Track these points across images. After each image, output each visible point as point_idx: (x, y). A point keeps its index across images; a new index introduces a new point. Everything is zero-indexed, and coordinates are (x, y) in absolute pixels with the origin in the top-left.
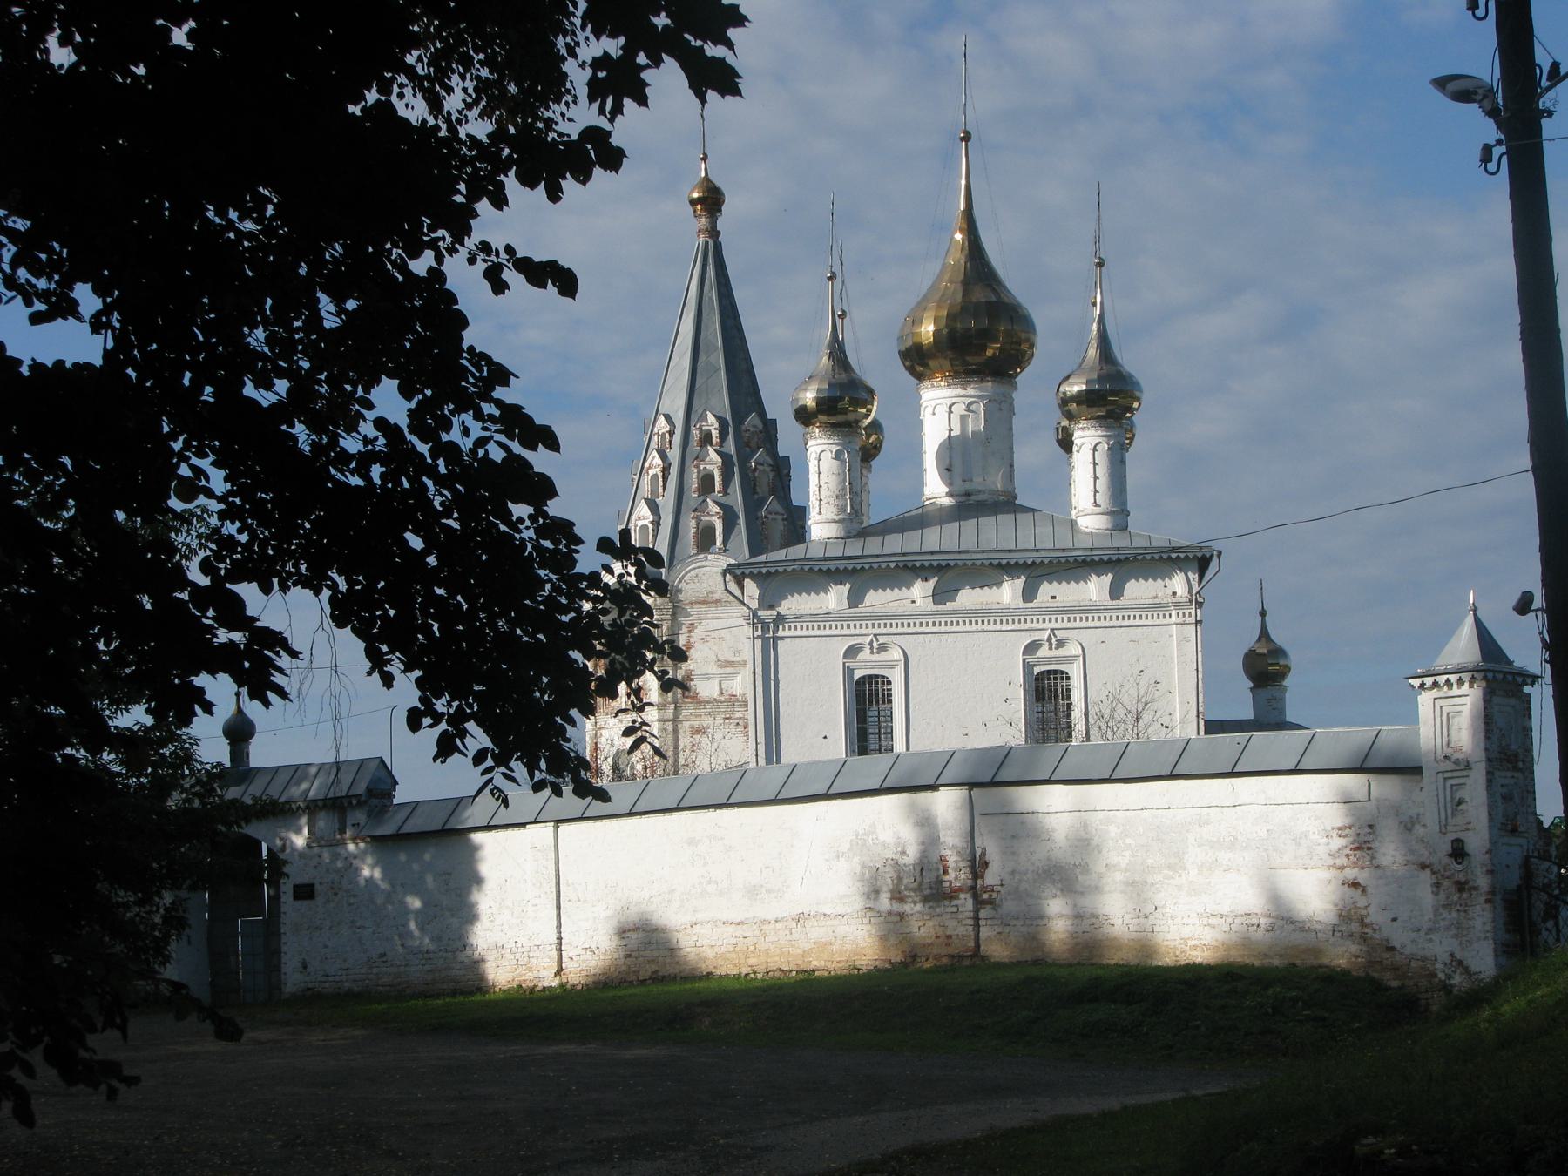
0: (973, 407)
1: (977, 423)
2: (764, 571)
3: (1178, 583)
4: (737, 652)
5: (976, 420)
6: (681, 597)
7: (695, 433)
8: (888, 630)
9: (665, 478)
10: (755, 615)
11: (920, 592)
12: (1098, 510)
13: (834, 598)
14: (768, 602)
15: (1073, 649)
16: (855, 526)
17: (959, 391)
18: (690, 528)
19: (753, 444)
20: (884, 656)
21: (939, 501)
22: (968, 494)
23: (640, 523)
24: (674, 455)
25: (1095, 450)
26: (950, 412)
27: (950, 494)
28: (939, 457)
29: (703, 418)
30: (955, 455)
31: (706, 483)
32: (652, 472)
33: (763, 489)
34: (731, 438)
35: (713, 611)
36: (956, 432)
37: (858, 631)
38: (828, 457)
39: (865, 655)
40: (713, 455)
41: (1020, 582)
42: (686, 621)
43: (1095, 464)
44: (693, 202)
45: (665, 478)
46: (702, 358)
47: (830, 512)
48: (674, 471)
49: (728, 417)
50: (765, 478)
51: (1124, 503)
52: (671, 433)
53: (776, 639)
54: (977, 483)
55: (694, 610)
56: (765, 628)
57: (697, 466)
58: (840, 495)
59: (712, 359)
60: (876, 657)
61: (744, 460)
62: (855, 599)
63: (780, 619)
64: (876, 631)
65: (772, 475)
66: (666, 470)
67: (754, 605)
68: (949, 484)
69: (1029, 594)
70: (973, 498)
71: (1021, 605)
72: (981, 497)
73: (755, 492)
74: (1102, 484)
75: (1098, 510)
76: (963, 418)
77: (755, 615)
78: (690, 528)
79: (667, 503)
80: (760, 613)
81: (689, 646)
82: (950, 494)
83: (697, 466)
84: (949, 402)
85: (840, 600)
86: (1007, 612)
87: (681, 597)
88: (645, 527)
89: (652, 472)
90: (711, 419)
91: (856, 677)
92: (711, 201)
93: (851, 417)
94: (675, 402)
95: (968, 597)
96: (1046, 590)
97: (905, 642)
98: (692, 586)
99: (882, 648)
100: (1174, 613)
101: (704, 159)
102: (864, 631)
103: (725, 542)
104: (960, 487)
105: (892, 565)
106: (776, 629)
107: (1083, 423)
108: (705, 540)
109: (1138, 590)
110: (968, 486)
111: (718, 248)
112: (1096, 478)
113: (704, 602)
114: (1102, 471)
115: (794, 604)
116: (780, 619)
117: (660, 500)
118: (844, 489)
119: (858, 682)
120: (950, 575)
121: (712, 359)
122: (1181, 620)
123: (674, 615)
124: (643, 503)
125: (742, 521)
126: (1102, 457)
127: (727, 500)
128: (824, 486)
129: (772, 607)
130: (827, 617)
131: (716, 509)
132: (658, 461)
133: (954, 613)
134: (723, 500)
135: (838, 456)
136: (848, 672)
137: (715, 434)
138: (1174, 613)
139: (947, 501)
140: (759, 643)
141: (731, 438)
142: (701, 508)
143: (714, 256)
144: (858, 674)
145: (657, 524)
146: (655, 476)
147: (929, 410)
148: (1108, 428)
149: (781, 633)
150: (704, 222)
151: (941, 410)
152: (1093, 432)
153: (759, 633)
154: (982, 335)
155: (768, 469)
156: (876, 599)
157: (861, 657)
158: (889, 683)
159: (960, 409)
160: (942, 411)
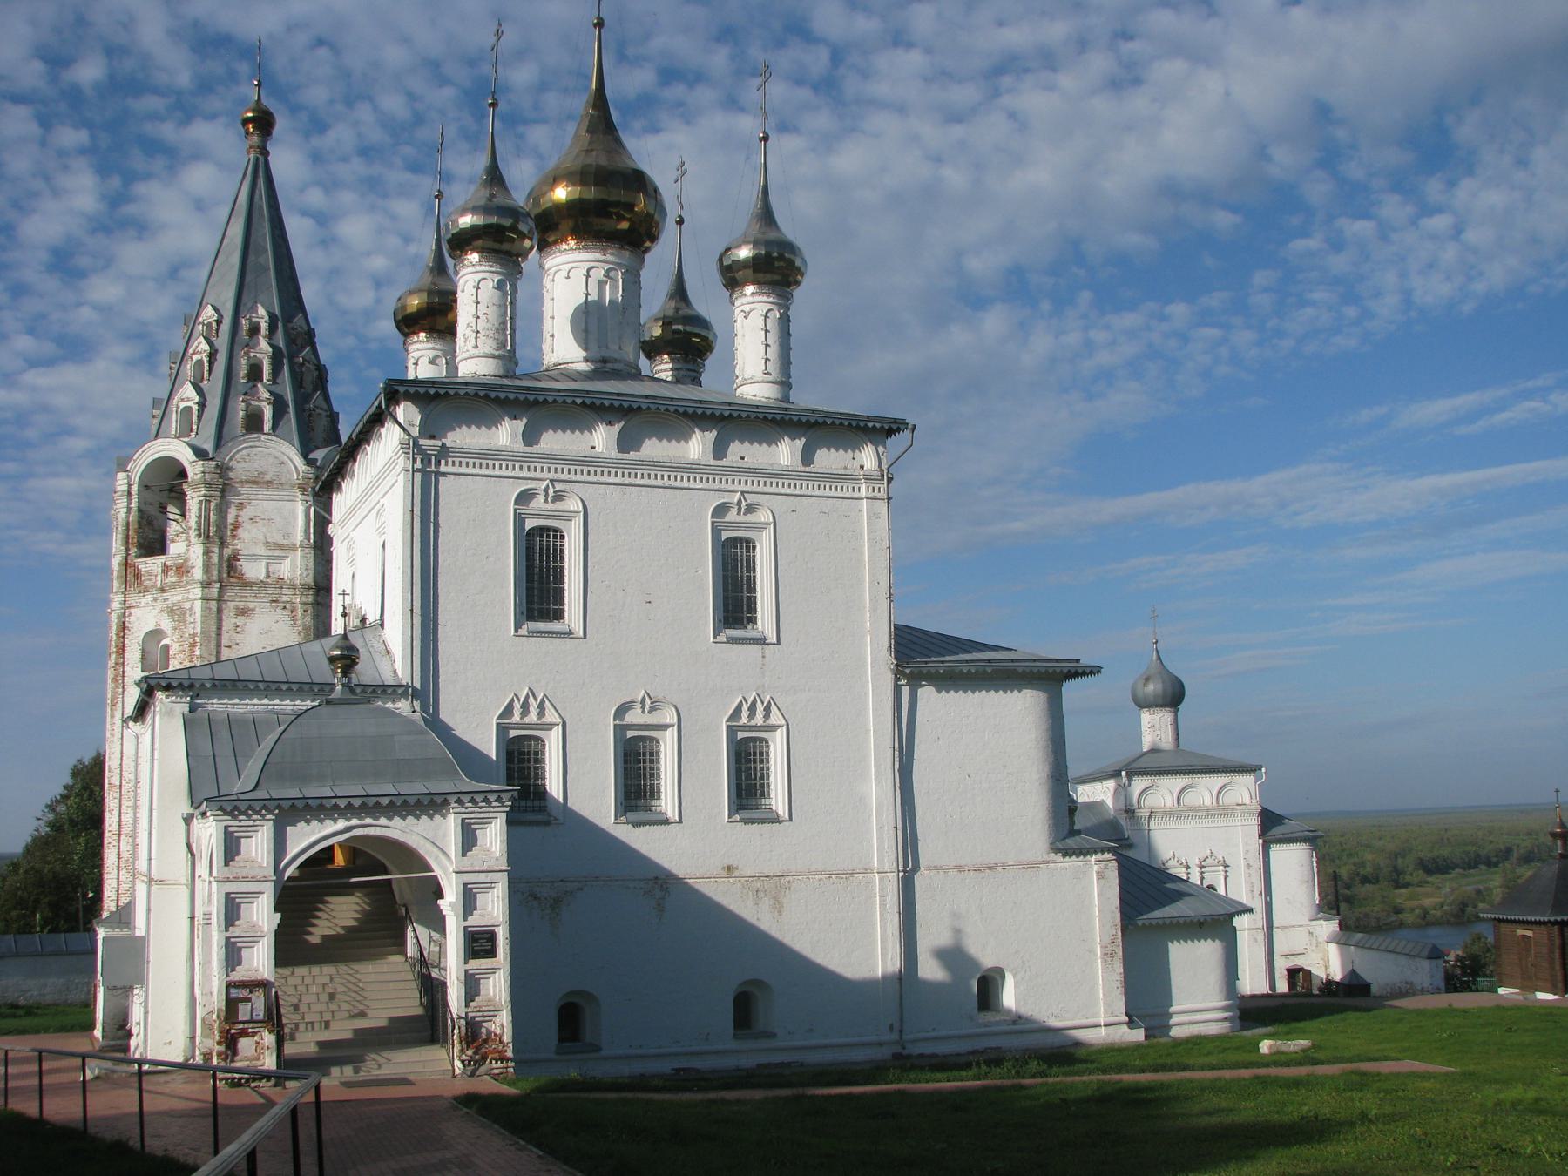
0: (612, 274)
1: (614, 293)
2: (432, 391)
3: (868, 457)
4: (287, 535)
5: (614, 288)
6: (231, 475)
8: (565, 476)
11: (602, 438)
13: (506, 434)
14: (429, 430)
15: (763, 516)
17: (598, 256)
18: (239, 411)
19: (299, 342)
20: (559, 506)
22: (604, 361)
23: (182, 405)
24: (222, 343)
25: (766, 317)
26: (588, 276)
27: (586, 360)
28: (574, 321)
30: (588, 320)
31: (255, 373)
32: (195, 358)
33: (308, 387)
34: (280, 333)
35: (264, 492)
36: (594, 297)
37: (531, 474)
38: (488, 287)
39: (538, 503)
40: (264, 344)
41: (711, 436)
42: (235, 499)
44: (246, 122)
45: (211, 364)
46: (252, 258)
47: (488, 346)
48: (222, 359)
49: (277, 311)
50: (310, 377)
52: (219, 322)
53: (439, 474)
54: (613, 351)
55: (245, 489)
56: (426, 460)
57: (247, 353)
58: (500, 329)
59: (261, 260)
60: (550, 506)
61: (292, 358)
62: (530, 437)
63: (444, 452)
64: (552, 475)
65: (316, 374)
66: (212, 356)
67: (415, 432)
68: (586, 349)
69: (719, 450)
70: (609, 365)
71: (712, 462)
72: (616, 366)
73: (301, 386)
74: (773, 352)
76: (601, 284)
78: (239, 411)
80: (422, 442)
81: (236, 526)
82: (586, 360)
83: (247, 353)
84: (588, 265)
85: (514, 435)
86: (695, 468)
87: (231, 475)
88: (189, 409)
89: (195, 358)
90: (262, 311)
91: (528, 527)
93: (515, 248)
95: (653, 448)
96: (736, 449)
97: (588, 492)
98: (242, 465)
99: (558, 497)
100: (864, 487)
102: (539, 475)
103: (274, 427)
105: (579, 401)
106: (438, 464)
107: (750, 289)
108: (253, 423)
109: (829, 459)
110: (607, 354)
112: (767, 345)
113: (255, 483)
114: (773, 339)
115: (463, 437)
116: (444, 452)
118: (504, 323)
119: (528, 534)
120: (639, 418)
121: (261, 260)
122: (870, 494)
123: (223, 491)
124: (189, 386)
125: (291, 410)
128: (483, 318)
129: (433, 437)
130: (498, 455)
131: (267, 395)
132: (205, 346)
133: (639, 464)
134: (273, 388)
135: (500, 286)
136: (520, 520)
137: (264, 326)
138: (864, 487)
139: (584, 367)
140: (418, 476)
141: (280, 333)
142: (250, 392)
143: (261, 173)
144: (530, 524)
145: (202, 405)
146: (200, 362)
148: (779, 296)
149: (443, 469)
150: (255, 139)
151: (569, 276)
152: (765, 299)
153: (418, 465)
154: (616, 210)
156: (553, 441)
157: (534, 504)
158: (563, 537)
159: (599, 274)
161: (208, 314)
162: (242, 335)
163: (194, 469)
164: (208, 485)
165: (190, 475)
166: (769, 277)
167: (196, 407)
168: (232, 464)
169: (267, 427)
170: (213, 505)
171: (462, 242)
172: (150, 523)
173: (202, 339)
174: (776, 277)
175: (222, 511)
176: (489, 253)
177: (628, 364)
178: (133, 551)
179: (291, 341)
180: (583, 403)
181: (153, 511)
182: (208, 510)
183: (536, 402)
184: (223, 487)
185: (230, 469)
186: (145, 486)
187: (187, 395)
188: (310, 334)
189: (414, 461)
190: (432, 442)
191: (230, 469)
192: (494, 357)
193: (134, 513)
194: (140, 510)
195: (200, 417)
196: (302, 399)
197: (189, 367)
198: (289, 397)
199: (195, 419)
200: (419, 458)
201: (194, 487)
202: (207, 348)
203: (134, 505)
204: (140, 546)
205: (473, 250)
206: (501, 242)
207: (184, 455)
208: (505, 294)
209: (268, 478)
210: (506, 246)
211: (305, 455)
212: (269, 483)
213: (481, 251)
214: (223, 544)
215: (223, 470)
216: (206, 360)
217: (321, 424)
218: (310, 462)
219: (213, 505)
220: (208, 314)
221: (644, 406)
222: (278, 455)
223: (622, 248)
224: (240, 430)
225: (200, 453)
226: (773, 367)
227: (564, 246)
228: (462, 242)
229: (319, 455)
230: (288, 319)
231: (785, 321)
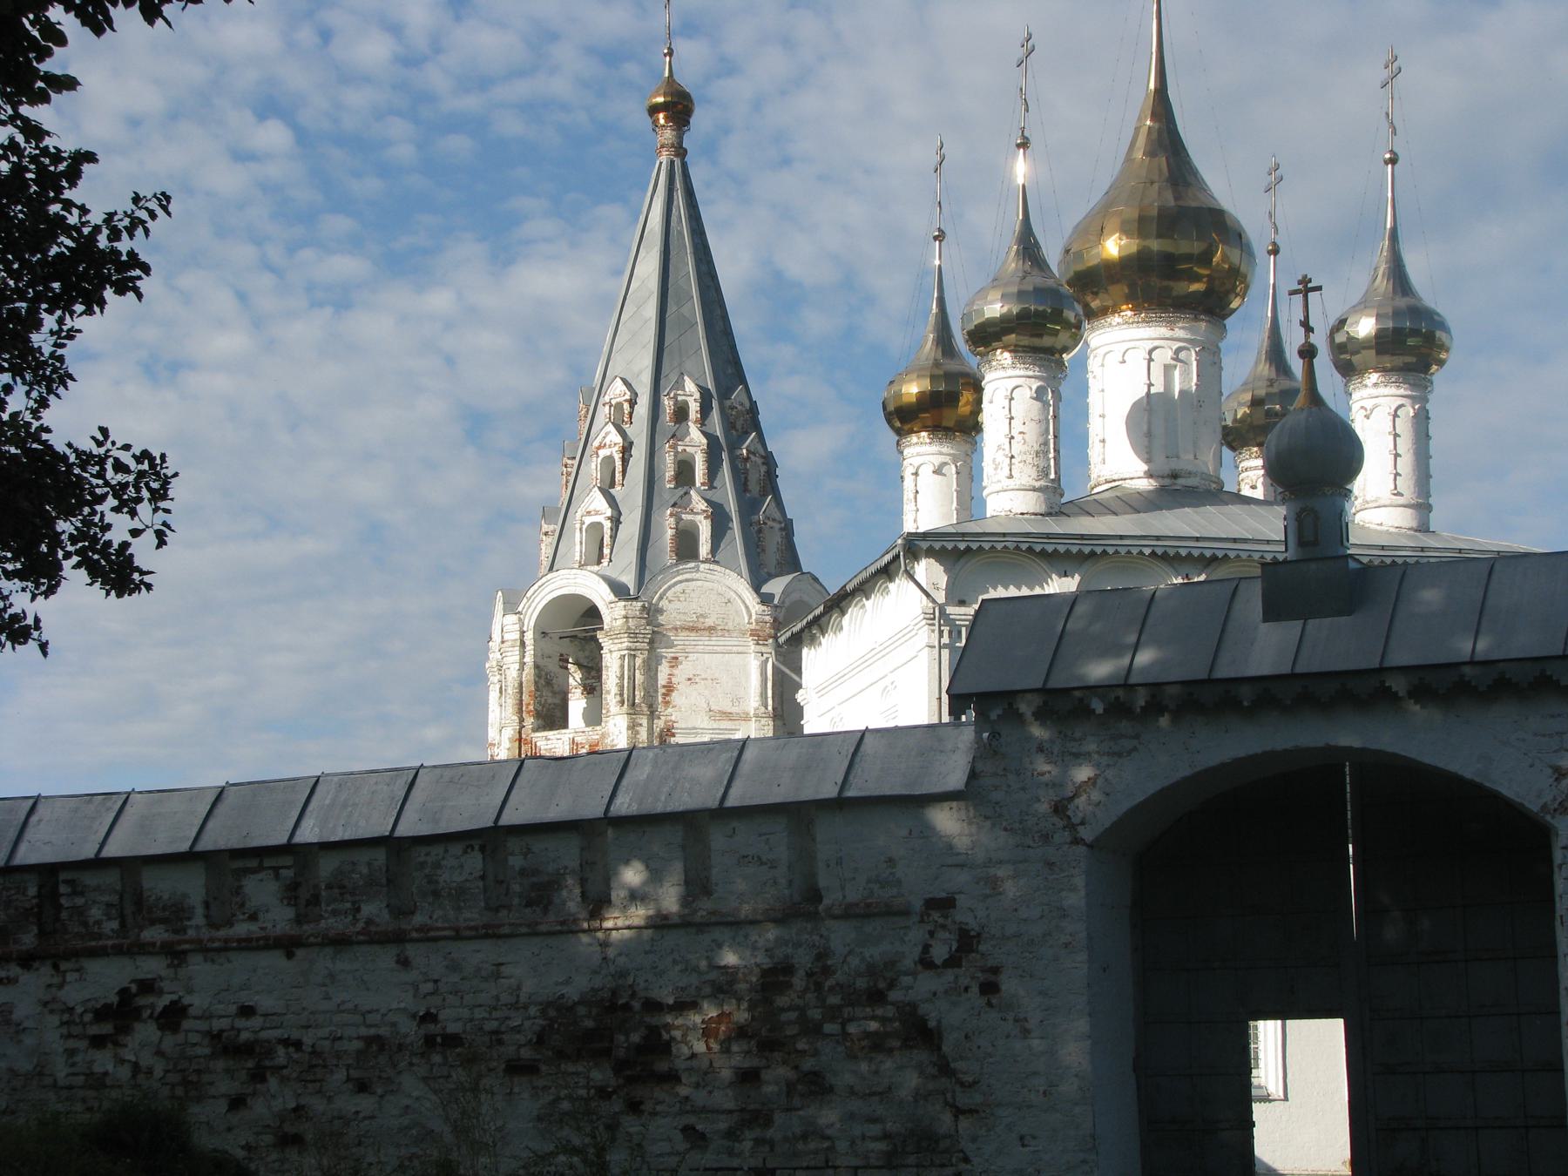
0: (1182, 355)
2: (962, 546)
4: (737, 700)
5: (1186, 374)
6: (661, 619)
7: (668, 404)
9: (625, 462)
10: (942, 613)
12: (1401, 500)
16: (1056, 499)
17: (1163, 331)
21: (1127, 484)
22: (1174, 476)
23: (588, 520)
24: (639, 430)
25: (1395, 416)
26: (1150, 360)
27: (1149, 475)
29: (679, 385)
30: (1152, 420)
31: (684, 472)
33: (754, 488)
34: (715, 415)
35: (704, 641)
36: (1158, 388)
38: (1025, 395)
43: (1396, 435)
44: (654, 110)
45: (625, 462)
47: (1026, 475)
49: (710, 385)
51: (1428, 495)
52: (632, 403)
54: (1185, 462)
55: (680, 639)
57: (674, 447)
58: (1042, 453)
59: (685, 310)
61: (733, 446)
65: (763, 469)
66: (626, 450)
67: (941, 597)
68: (1148, 461)
70: (1181, 481)
74: (1406, 464)
75: (1401, 500)
76: (1168, 369)
77: (942, 613)
79: (631, 492)
80: (950, 610)
81: (670, 688)
82: (1149, 475)
83: (674, 447)
87: (661, 619)
88: (597, 527)
89: (603, 453)
92: (679, 108)
94: (635, 360)
101: (670, 53)
103: (714, 549)
104: (1165, 466)
105: (1147, 551)
108: (686, 547)
110: (1175, 465)
111: (684, 166)
112: (1397, 455)
113: (692, 629)
114: (1406, 445)
117: (617, 491)
118: (1046, 443)
121: (685, 310)
123: (652, 642)
125: (735, 524)
126: (1405, 426)
127: (716, 496)
128: (1018, 438)
129: (962, 603)
131: (702, 506)
132: (615, 437)
134: (709, 495)
135: (1039, 395)
137: (694, 408)
139: (1146, 485)
140: (946, 653)
141: (715, 415)
142: (681, 504)
145: (616, 521)
147: (1099, 360)
148: (1413, 386)
150: (668, 135)
151: (1127, 357)
152: (1392, 390)
153: (946, 640)
155: (759, 461)
159: (1164, 356)
160: (1138, 359)
161: (617, 391)
162: (665, 421)
163: (613, 613)
164: (633, 635)
165: (607, 619)
166: (1399, 361)
167: (607, 525)
168: (663, 604)
169: (704, 549)
170: (639, 661)
171: (986, 336)
172: (549, 683)
173: (610, 427)
174: (1411, 359)
175: (651, 668)
176: (1023, 352)
177: (1205, 476)
178: (529, 721)
179: (729, 425)
180: (1153, 554)
181: (552, 666)
182: (632, 669)
183: (1093, 554)
184: (652, 637)
185: (660, 611)
186: (542, 634)
187: (595, 506)
188: (753, 410)
189: (941, 632)
190: (962, 610)
191: (660, 611)
192: (1034, 490)
193: (529, 671)
194: (537, 666)
195: (614, 537)
196: (748, 507)
197: (593, 468)
198: (732, 507)
199: (607, 540)
200: (946, 630)
201: (614, 636)
202: (619, 439)
203: (529, 659)
204: (537, 715)
205: (1005, 348)
206: (1040, 336)
207: (600, 594)
208: (1046, 404)
209: (709, 622)
210: (1047, 341)
211: (756, 587)
212: (711, 629)
213: (1014, 349)
214: (653, 714)
215: (651, 613)
216: (617, 457)
217: (773, 540)
218: (766, 599)
219: (639, 661)
220: (617, 391)
221: (1232, 555)
222: (721, 592)
223: (1196, 319)
224: (670, 559)
225: (619, 590)
226: (1407, 485)
227: (1116, 319)
228: (986, 336)
229: (776, 586)
230: (724, 394)
231: (1422, 421)
